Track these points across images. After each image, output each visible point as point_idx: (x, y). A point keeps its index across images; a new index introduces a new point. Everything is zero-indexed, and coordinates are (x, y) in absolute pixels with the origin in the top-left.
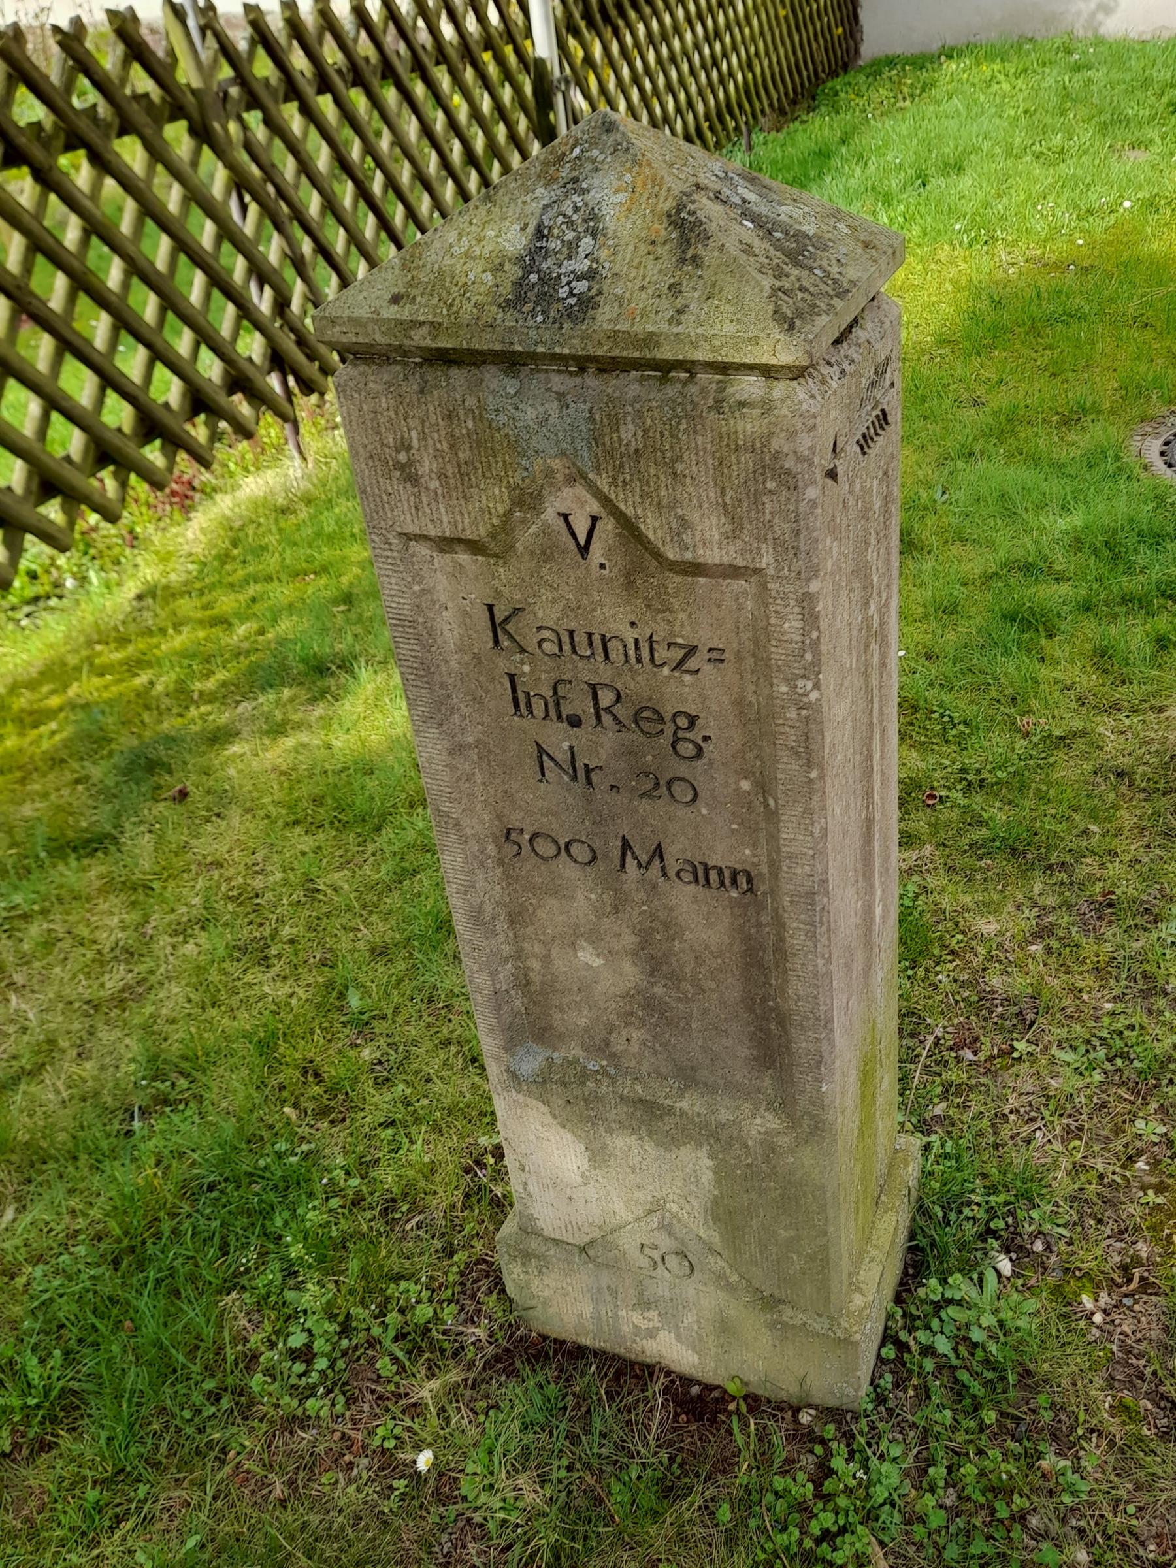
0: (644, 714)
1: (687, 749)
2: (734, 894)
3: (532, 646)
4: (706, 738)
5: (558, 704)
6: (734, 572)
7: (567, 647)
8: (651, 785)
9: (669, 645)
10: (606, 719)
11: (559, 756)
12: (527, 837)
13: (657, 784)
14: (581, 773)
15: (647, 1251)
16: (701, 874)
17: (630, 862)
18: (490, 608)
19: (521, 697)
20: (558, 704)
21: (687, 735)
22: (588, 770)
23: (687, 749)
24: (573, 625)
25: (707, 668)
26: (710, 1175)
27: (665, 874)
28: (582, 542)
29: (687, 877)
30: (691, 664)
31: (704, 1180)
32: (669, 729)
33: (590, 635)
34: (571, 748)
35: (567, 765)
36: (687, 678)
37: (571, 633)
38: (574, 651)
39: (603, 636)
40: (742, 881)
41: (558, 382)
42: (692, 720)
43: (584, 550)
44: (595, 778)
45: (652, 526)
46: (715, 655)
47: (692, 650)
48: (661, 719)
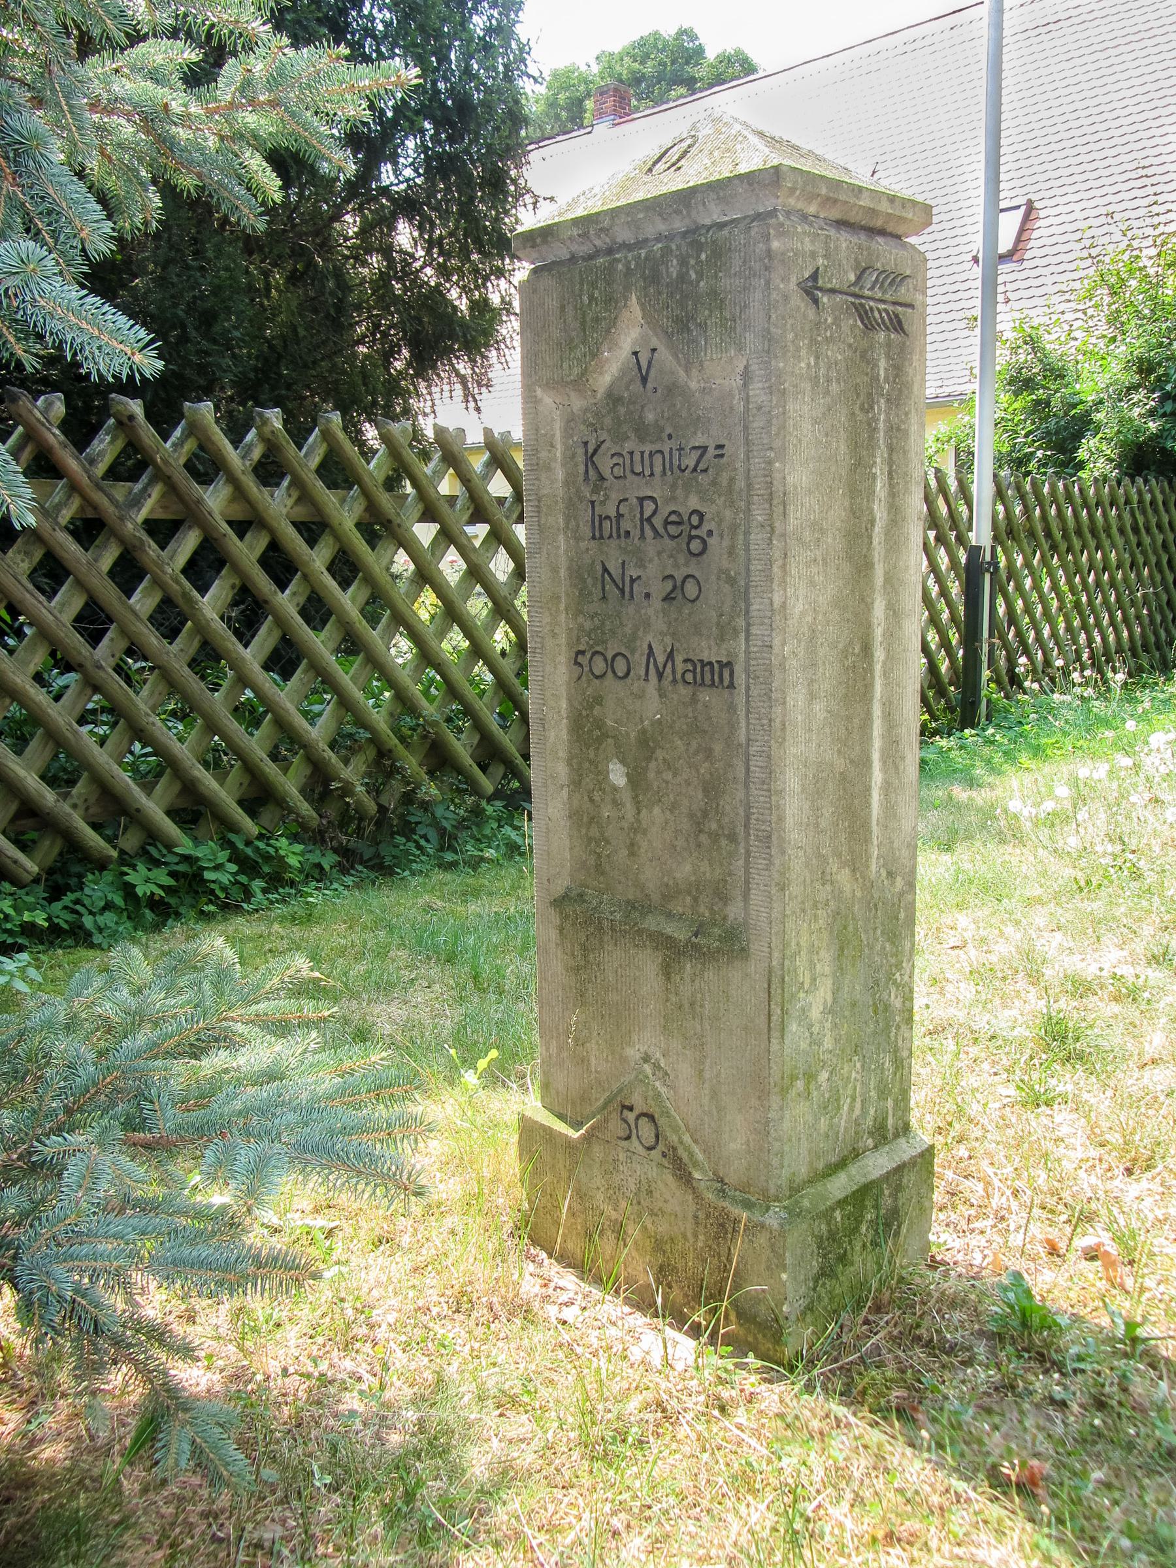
1: (695, 546)
3: (607, 473)
10: (647, 527)
12: (588, 656)
13: (675, 587)
22: (632, 581)
23: (695, 546)
29: (689, 677)
33: (642, 453)
37: (631, 453)
42: (702, 516)
43: (644, 380)
46: (720, 452)
47: (705, 449)
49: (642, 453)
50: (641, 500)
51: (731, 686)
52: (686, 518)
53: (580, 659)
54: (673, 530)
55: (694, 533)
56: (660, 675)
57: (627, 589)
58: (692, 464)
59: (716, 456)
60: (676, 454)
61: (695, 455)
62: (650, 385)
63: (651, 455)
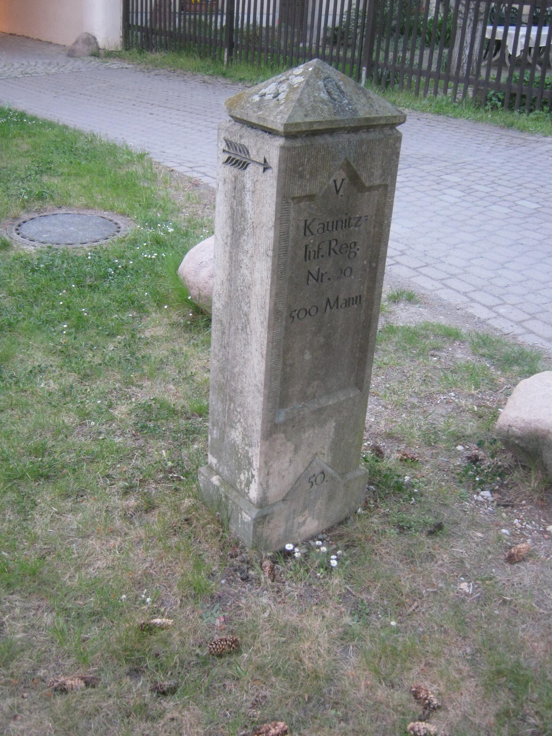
2: (355, 306)
3: (315, 232)
4: (358, 249)
5: (318, 252)
6: (380, 186)
7: (326, 228)
10: (332, 251)
16: (348, 302)
17: (328, 307)
18: (306, 221)
19: (308, 252)
20: (318, 252)
24: (328, 220)
26: (333, 430)
27: (337, 308)
29: (344, 306)
30: (359, 224)
31: (331, 434)
35: (316, 277)
36: (357, 229)
37: (328, 223)
41: (346, 136)
42: (355, 243)
43: (338, 191)
44: (324, 277)
45: (364, 177)
47: (361, 217)
48: (347, 247)
52: (349, 245)
56: (331, 308)
63: (337, 222)
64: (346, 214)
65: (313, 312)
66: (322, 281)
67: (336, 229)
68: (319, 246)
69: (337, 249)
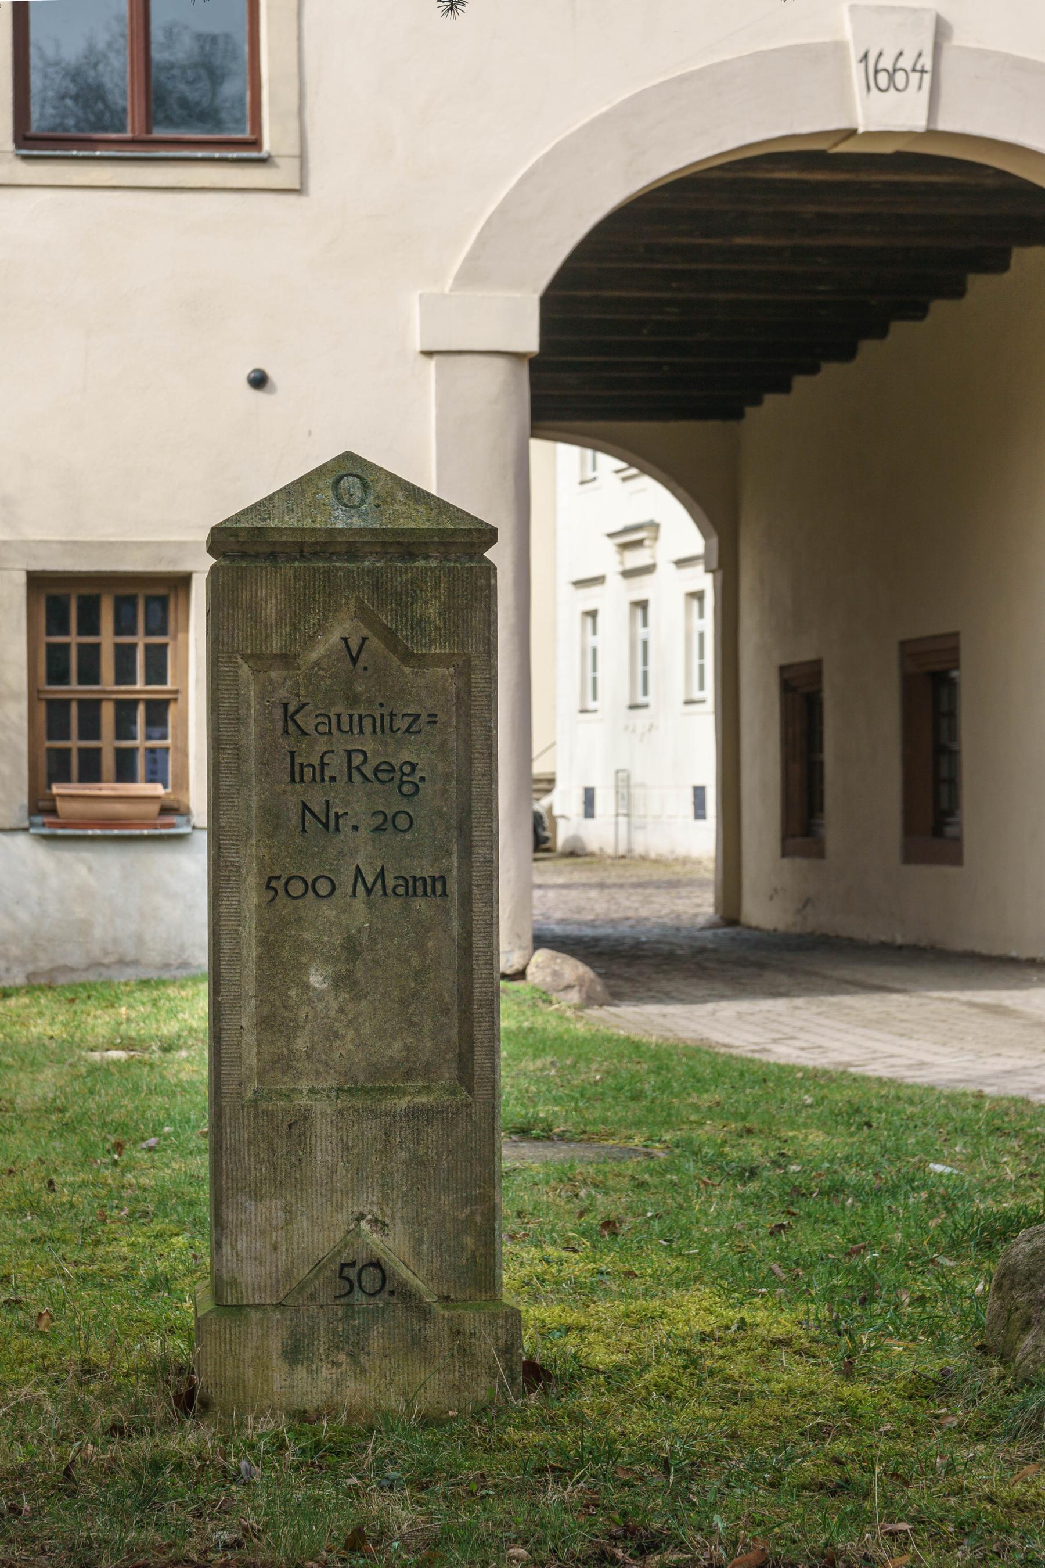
0: (382, 768)
3: (310, 729)
4: (423, 779)
8: (381, 818)
9: (403, 716)
10: (355, 773)
11: (316, 809)
12: (283, 881)
13: (385, 820)
14: (332, 823)
15: (345, 1274)
18: (286, 706)
19: (297, 768)
21: (410, 779)
23: (407, 789)
25: (428, 728)
27: (385, 893)
28: (354, 655)
29: (401, 891)
32: (397, 775)
33: (351, 716)
34: (327, 802)
37: (339, 716)
38: (339, 728)
39: (360, 716)
40: (439, 887)
42: (413, 766)
43: (354, 660)
44: (341, 821)
46: (433, 719)
47: (419, 716)
48: (394, 770)
49: (351, 716)
50: (349, 753)
51: (444, 893)
52: (397, 768)
53: (273, 884)
54: (382, 776)
55: (405, 778)
56: (369, 891)
57: (332, 823)
58: (404, 727)
59: (429, 722)
60: (387, 719)
61: (408, 721)
62: (361, 664)
64: (381, 705)
65: (323, 888)
66: (337, 829)
67: (361, 731)
68: (322, 758)
69: (368, 770)
